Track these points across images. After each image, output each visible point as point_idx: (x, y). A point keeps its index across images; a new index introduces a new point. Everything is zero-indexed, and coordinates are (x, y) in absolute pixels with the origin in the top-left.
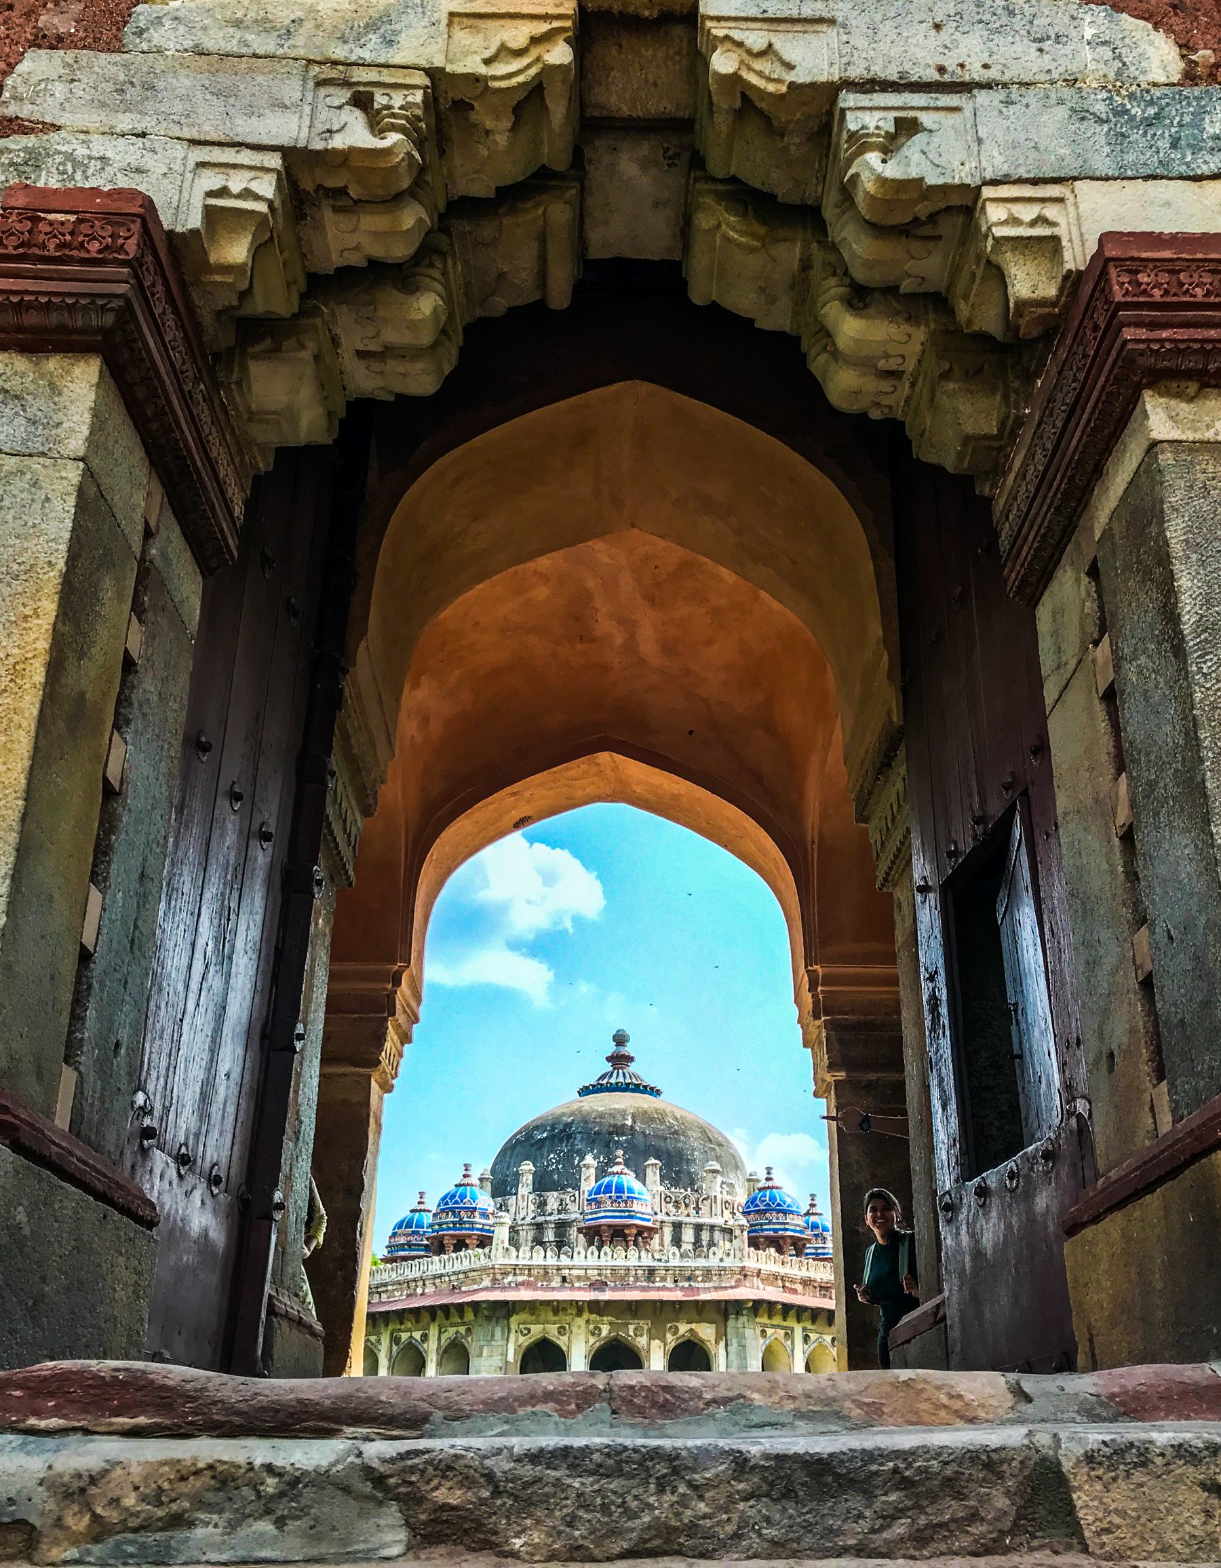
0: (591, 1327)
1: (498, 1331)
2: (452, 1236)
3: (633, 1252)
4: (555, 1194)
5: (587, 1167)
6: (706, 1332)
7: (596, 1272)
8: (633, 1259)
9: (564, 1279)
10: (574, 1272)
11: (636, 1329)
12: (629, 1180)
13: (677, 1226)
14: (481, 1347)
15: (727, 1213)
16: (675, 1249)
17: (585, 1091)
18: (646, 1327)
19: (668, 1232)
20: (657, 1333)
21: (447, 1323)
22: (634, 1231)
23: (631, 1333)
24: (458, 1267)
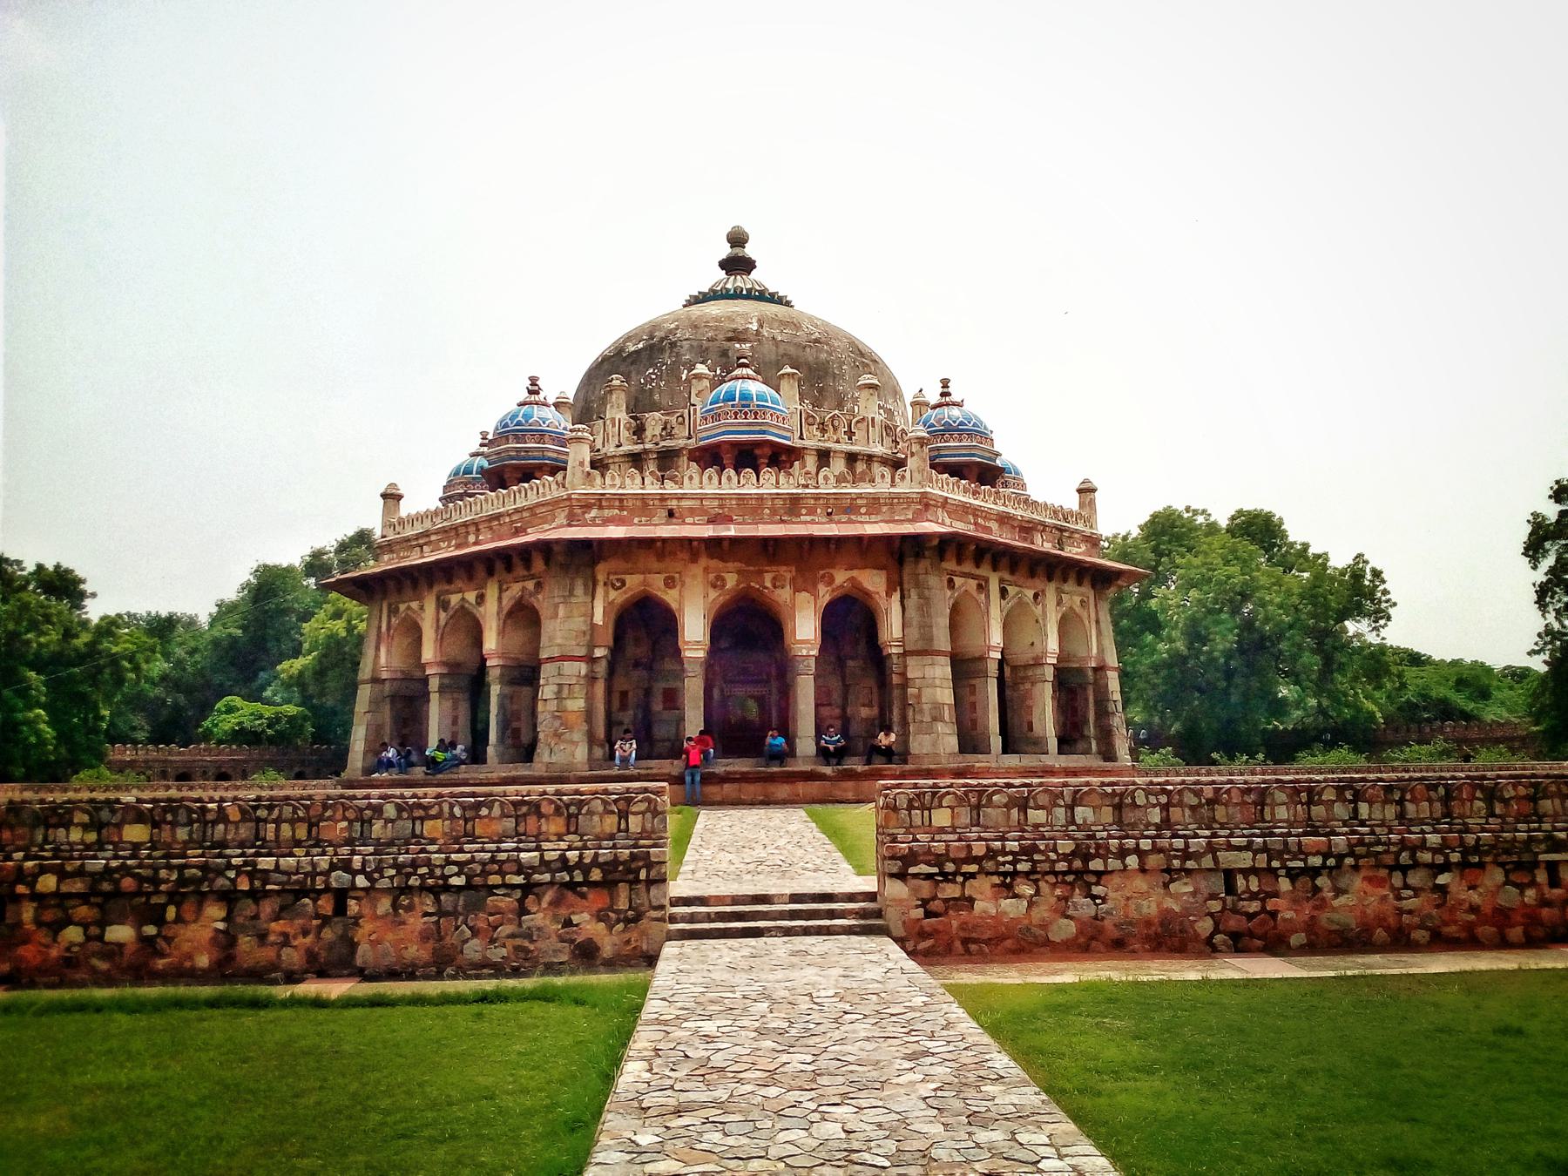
0: (712, 576)
2: (516, 468)
3: (768, 474)
4: (657, 414)
5: (699, 377)
7: (716, 503)
9: (671, 514)
11: (774, 578)
12: (755, 387)
13: (824, 457)
14: (556, 606)
15: (888, 440)
18: (788, 576)
19: (811, 462)
20: (804, 583)
21: (509, 577)
22: (767, 451)
23: (768, 584)
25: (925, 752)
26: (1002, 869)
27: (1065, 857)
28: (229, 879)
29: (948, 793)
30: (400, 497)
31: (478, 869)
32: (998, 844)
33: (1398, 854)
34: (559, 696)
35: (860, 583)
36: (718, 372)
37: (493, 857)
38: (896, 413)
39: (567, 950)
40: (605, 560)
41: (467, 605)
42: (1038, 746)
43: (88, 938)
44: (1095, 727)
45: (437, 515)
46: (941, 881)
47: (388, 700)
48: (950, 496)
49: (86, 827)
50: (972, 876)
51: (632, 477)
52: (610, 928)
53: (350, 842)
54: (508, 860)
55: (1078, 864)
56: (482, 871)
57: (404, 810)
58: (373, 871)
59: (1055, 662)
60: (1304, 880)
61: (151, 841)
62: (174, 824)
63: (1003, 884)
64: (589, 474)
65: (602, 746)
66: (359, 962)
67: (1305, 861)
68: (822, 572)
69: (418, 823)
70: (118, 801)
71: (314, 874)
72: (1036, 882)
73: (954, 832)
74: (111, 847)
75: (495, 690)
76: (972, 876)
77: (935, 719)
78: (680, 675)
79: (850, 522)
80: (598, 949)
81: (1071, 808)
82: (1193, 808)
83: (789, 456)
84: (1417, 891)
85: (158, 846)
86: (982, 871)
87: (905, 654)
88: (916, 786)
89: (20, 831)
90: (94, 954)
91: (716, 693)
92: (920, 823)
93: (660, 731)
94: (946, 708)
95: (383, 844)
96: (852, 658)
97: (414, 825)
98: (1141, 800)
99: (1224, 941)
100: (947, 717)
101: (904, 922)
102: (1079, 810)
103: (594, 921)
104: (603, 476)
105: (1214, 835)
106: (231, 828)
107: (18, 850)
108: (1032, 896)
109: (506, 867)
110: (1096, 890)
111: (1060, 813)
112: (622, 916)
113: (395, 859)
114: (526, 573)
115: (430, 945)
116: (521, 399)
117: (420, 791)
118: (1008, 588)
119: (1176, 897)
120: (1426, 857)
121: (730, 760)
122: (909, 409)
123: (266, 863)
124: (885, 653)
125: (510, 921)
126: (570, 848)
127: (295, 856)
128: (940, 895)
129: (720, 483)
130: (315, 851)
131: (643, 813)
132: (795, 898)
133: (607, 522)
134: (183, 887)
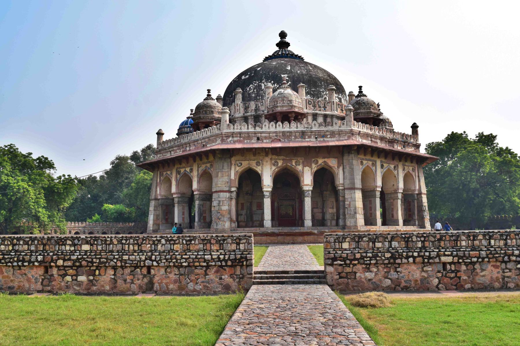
0: (273, 161)
1: (225, 165)
2: (203, 123)
3: (293, 124)
5: (268, 88)
6: (333, 163)
8: (293, 128)
9: (258, 139)
10: (263, 135)
11: (296, 162)
12: (289, 91)
13: (315, 116)
15: (339, 110)
16: (315, 122)
17: (266, 59)
18: (301, 161)
19: (310, 118)
22: (294, 115)
24: (205, 135)
25: (352, 225)
26: (366, 262)
27: (388, 259)
28: (114, 262)
29: (348, 237)
30: (163, 134)
31: (192, 260)
32: (364, 254)
33: (504, 257)
34: (219, 205)
35: (328, 163)
36: (276, 85)
37: (196, 257)
38: (342, 99)
39: (221, 287)
40: (235, 156)
41: (186, 172)
42: (395, 223)
43: (73, 280)
44: (418, 216)
45: (176, 140)
46: (345, 267)
47: (160, 206)
48: (361, 130)
49: (70, 245)
50: (355, 265)
51: (244, 126)
52: (234, 280)
53: (151, 251)
54: (201, 258)
55: (392, 261)
56: (193, 261)
57: (168, 241)
58: (159, 260)
59: (402, 191)
60: (470, 266)
61: (90, 250)
62: (97, 245)
63: (366, 268)
64: (228, 125)
65: (234, 222)
66: (155, 289)
67: (471, 260)
68: (313, 160)
69: (172, 245)
70: (80, 238)
71: (140, 261)
72: (377, 267)
73: (350, 250)
74: (78, 252)
75: (197, 203)
76: (355, 265)
77: (355, 213)
78: (263, 196)
79: (324, 141)
80: (230, 287)
81: (390, 242)
82: (433, 242)
83: (302, 117)
84: (510, 270)
85: (93, 251)
86: (358, 263)
87: (344, 189)
88: (337, 235)
89: (51, 246)
90: (75, 285)
91: (276, 204)
92: (338, 247)
93: (255, 218)
94: (360, 209)
95: (162, 252)
96: (326, 191)
97: (171, 246)
98: (414, 239)
99: (442, 287)
100: (360, 212)
101: (332, 280)
102: (393, 243)
103: (229, 278)
104: (234, 125)
105: (440, 251)
106: (115, 246)
107: (51, 252)
108: (376, 271)
109: (201, 260)
110: (398, 269)
111: (387, 244)
112: (238, 277)
113: (166, 256)
114: (207, 161)
115: (177, 284)
116: (205, 98)
117: (173, 235)
118: (384, 164)
119: (427, 271)
120: (514, 258)
121: (281, 228)
122: (348, 97)
123: (125, 257)
124: (337, 189)
125: (202, 277)
126: (221, 254)
127: (134, 255)
128: (344, 271)
129: (276, 127)
130: (140, 254)
131: (244, 243)
132: (296, 272)
133: (235, 142)
134: (101, 264)
